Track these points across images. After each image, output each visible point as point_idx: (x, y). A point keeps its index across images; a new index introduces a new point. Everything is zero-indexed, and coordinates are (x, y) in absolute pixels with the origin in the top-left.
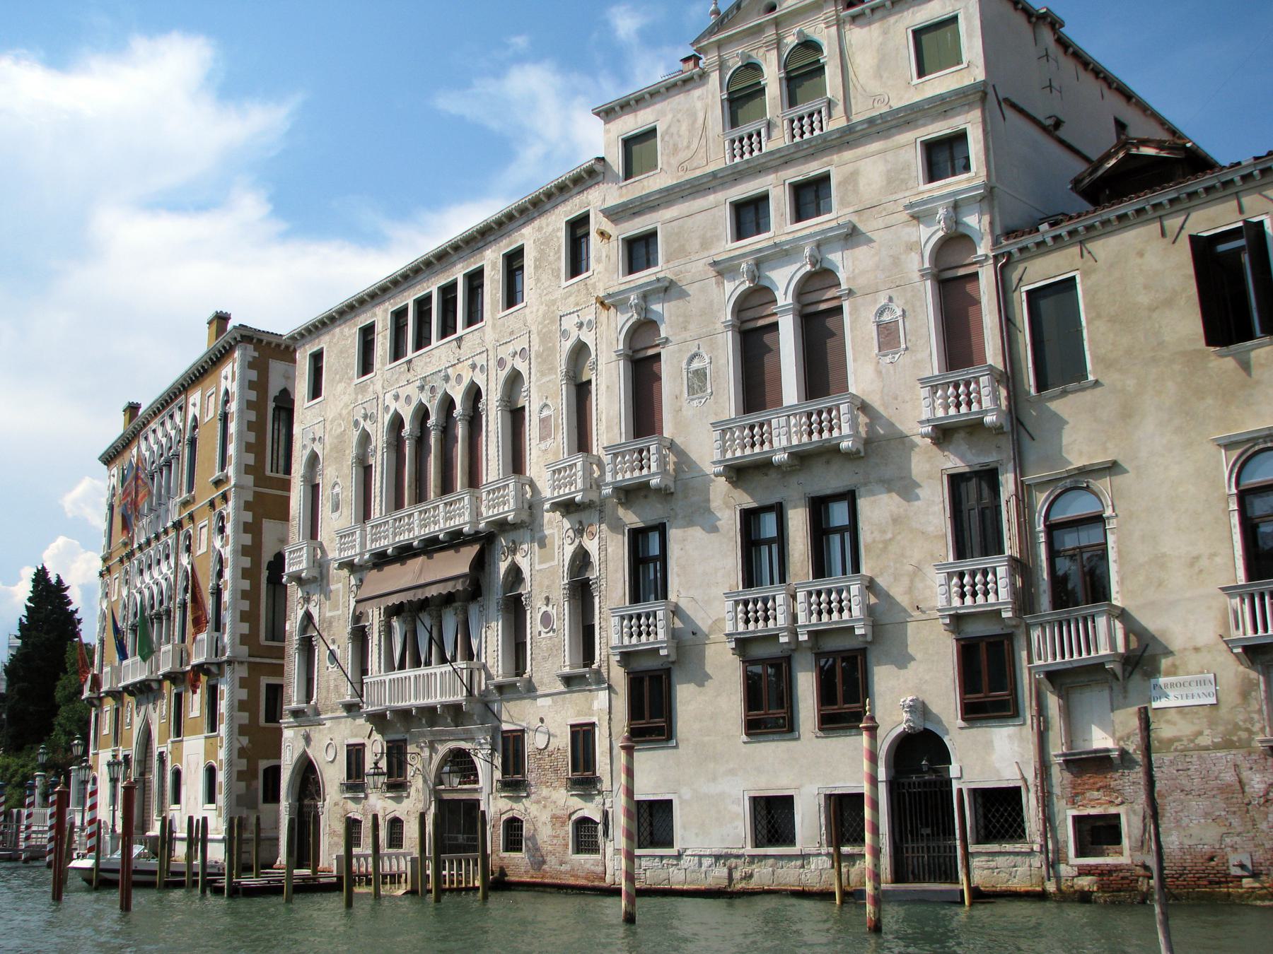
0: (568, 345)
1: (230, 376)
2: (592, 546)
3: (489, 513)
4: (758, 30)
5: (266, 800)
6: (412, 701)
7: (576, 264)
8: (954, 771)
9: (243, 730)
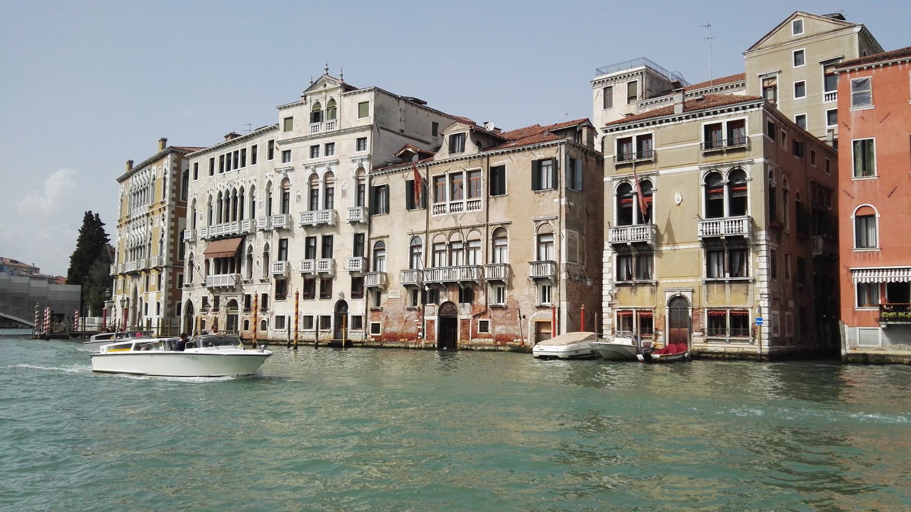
0: (267, 181)
1: (167, 163)
2: (270, 243)
3: (244, 229)
4: (321, 92)
6: (221, 285)
7: (271, 156)
9: (170, 290)
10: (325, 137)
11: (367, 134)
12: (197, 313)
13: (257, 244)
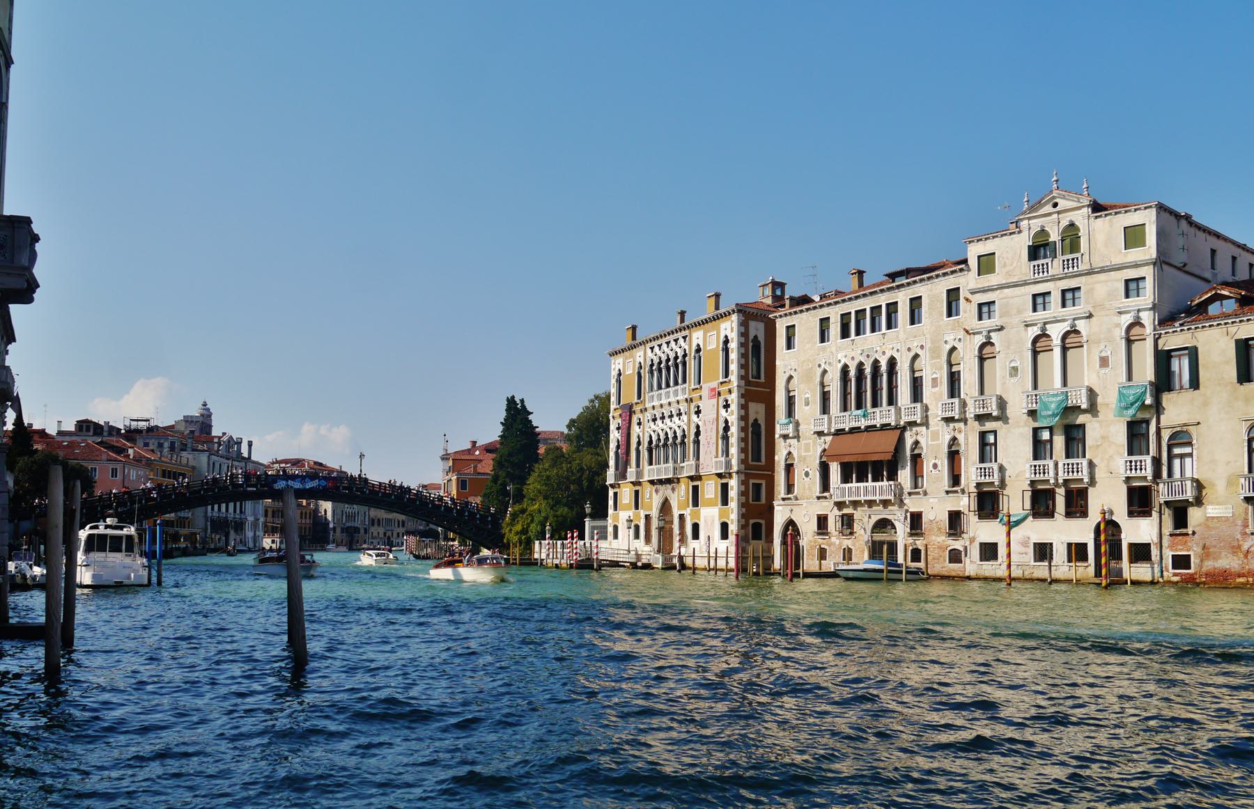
0: (948, 347)
1: (730, 327)
2: (961, 437)
5: (754, 538)
8: (1123, 536)
10: (1060, 279)
11: (1148, 272)
12: (808, 536)
13: (932, 442)
